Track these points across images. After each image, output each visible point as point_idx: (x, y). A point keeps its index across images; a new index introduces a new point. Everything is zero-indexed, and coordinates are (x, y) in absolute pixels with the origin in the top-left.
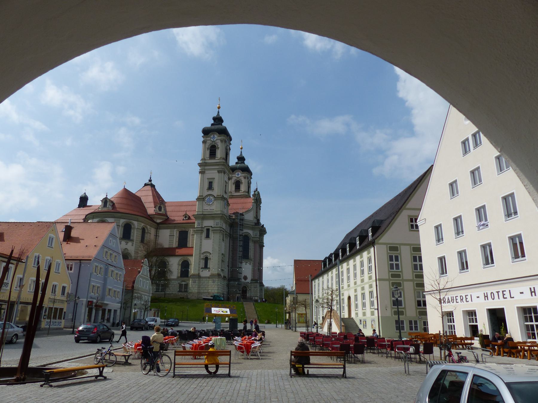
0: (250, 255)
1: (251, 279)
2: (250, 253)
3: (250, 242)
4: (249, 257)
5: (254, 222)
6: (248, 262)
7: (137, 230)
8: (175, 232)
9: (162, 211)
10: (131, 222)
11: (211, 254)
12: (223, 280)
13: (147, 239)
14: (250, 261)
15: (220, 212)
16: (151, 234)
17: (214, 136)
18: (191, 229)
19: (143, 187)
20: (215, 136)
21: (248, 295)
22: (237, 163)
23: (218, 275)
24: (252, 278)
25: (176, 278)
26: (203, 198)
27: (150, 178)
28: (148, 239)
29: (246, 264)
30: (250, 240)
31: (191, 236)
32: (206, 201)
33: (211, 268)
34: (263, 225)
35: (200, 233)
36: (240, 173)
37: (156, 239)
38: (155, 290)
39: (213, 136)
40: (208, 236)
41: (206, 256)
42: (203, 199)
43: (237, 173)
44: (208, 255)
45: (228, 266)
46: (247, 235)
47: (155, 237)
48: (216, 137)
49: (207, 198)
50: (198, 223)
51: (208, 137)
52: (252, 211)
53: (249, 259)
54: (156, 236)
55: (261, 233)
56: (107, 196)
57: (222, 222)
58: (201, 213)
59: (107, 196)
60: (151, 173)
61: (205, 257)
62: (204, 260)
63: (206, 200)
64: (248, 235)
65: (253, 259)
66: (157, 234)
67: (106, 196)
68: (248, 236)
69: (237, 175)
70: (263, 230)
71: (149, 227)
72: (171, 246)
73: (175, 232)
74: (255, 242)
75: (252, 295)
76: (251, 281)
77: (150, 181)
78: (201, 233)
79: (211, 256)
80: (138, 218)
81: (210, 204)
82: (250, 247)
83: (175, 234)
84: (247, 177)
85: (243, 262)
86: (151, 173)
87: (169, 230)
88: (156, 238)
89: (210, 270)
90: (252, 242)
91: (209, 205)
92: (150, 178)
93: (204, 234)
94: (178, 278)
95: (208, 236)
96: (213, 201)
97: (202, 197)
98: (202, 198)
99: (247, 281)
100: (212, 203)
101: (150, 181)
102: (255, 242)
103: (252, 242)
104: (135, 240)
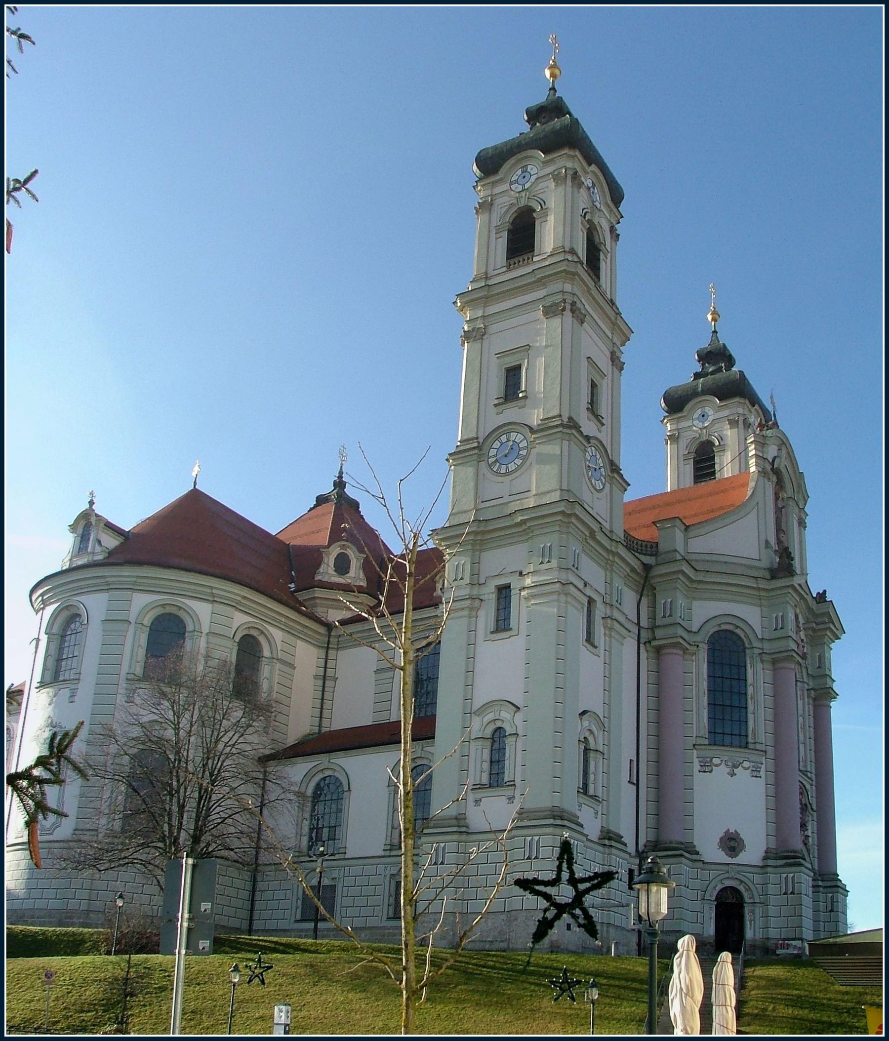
0: (751, 724)
1: (765, 849)
2: (751, 717)
3: (748, 662)
4: (750, 740)
5: (765, 564)
6: (746, 764)
9: (352, 573)
10: (180, 608)
11: (519, 708)
12: (601, 848)
13: (271, 689)
14: (753, 758)
15: (558, 493)
16: (292, 666)
19: (311, 509)
21: (749, 934)
22: (697, 376)
23: (554, 817)
24: (773, 846)
25: (382, 853)
26: (479, 448)
27: (340, 477)
28: (276, 687)
29: (733, 775)
30: (748, 651)
32: (491, 461)
33: (518, 782)
34: (822, 596)
35: (466, 613)
36: (709, 411)
37: (323, 691)
38: (299, 917)
40: (502, 624)
41: (499, 724)
42: (476, 451)
43: (699, 411)
44: (506, 715)
45: (637, 785)
46: (730, 627)
47: (320, 683)
49: (497, 444)
50: (457, 566)
52: (753, 516)
53: (751, 746)
54: (324, 678)
55: (814, 630)
56: (91, 503)
57: (575, 547)
59: (91, 503)
60: (343, 457)
61: (492, 727)
62: (488, 743)
63: (493, 452)
64: (737, 627)
65: (770, 751)
66: (330, 672)
67: (88, 506)
68: (738, 631)
69: (698, 419)
70: (824, 614)
71: (278, 635)
74: (777, 661)
75: (773, 933)
76: (765, 858)
77: (340, 484)
78: (473, 611)
79: (519, 717)
80: (212, 588)
81: (512, 467)
82: (750, 690)
84: (741, 419)
85: (716, 761)
86: (343, 457)
88: (324, 687)
89: (517, 795)
90: (762, 661)
91: (508, 473)
92: (341, 473)
93: (487, 616)
94: (387, 853)
95: (502, 624)
96: (524, 452)
97: (476, 445)
98: (474, 448)
99: (742, 858)
100: (518, 462)
101: (340, 484)
102: (774, 662)
103: (760, 666)
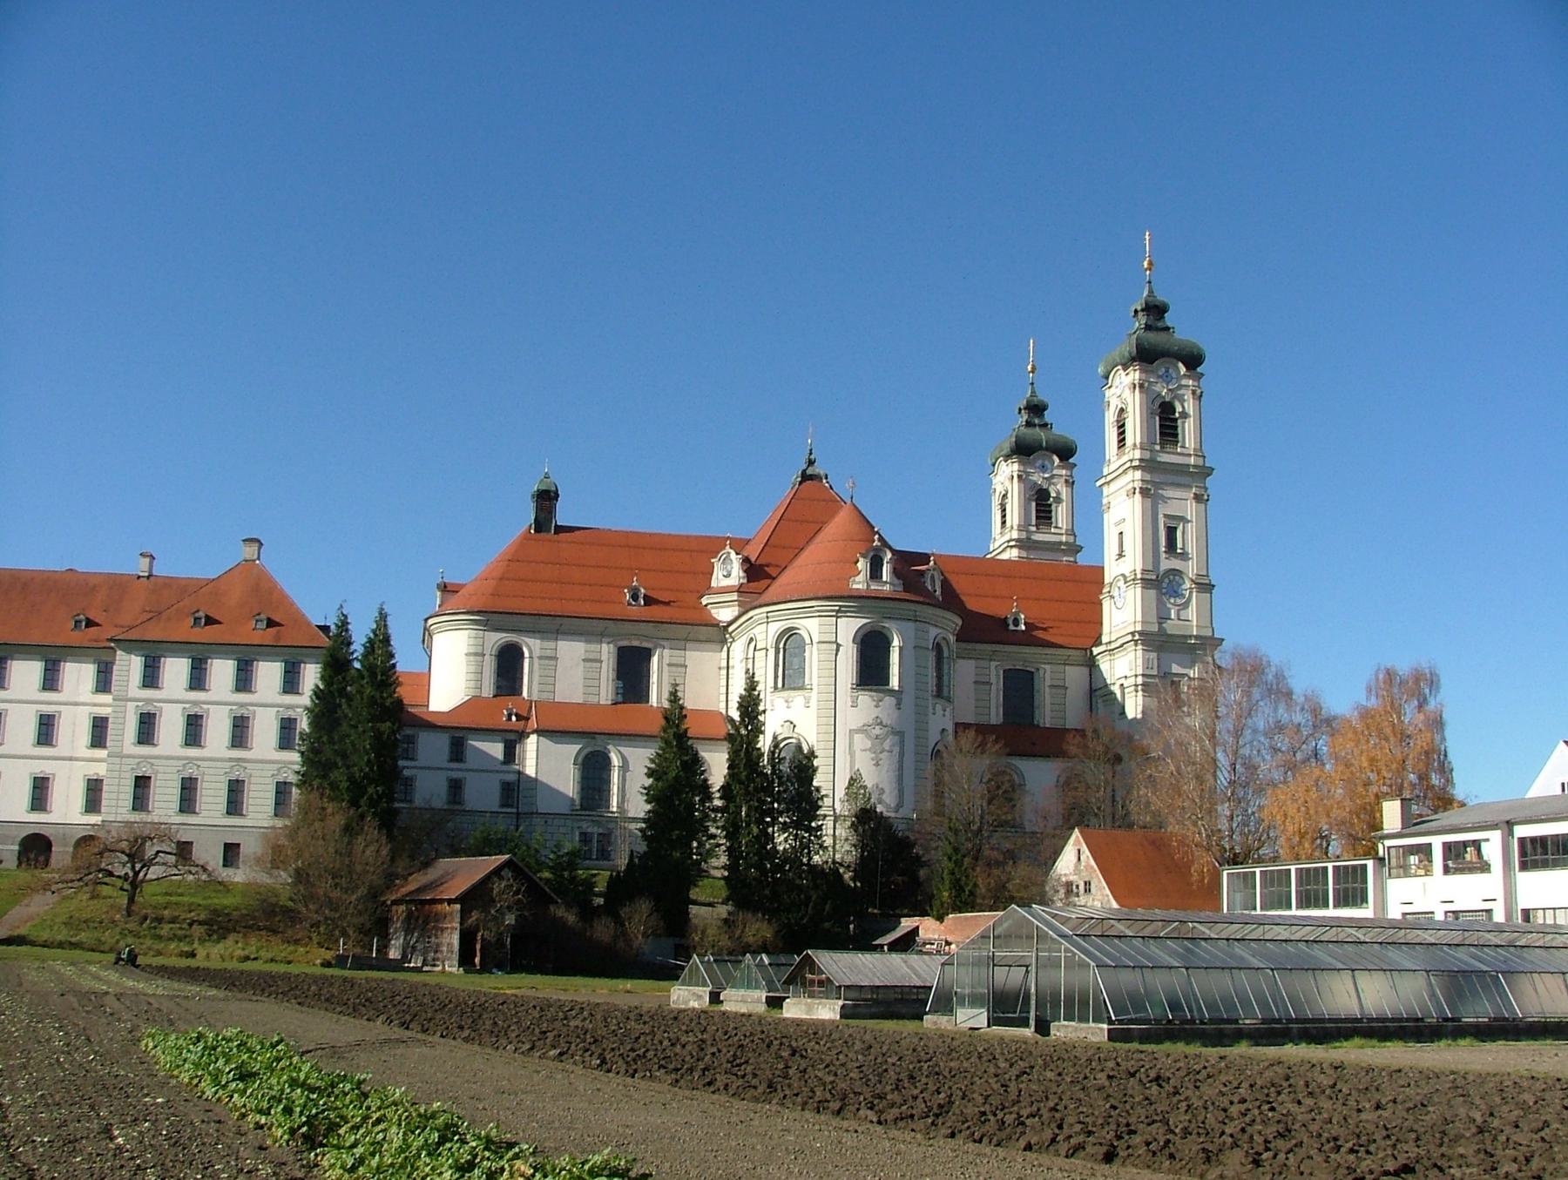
7: (818, 650)
8: (993, 672)
17: (1167, 371)
18: (1047, 667)
20: (1170, 371)
31: (1047, 689)
32: (1164, 591)
39: (1163, 370)
48: (1174, 375)
51: (1152, 372)
58: (1155, 628)
72: (983, 720)
73: (993, 672)
83: (993, 680)
87: (973, 662)
104: (815, 687)
